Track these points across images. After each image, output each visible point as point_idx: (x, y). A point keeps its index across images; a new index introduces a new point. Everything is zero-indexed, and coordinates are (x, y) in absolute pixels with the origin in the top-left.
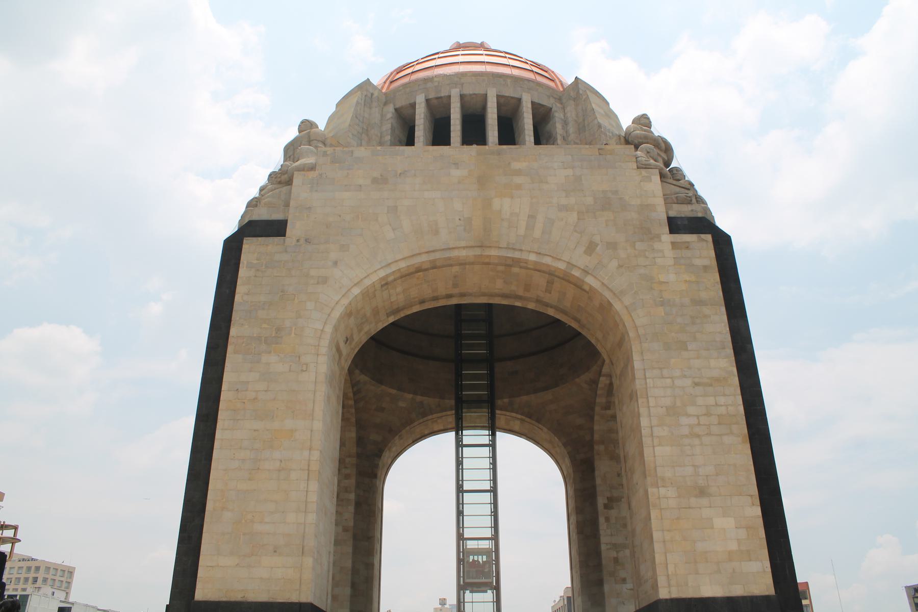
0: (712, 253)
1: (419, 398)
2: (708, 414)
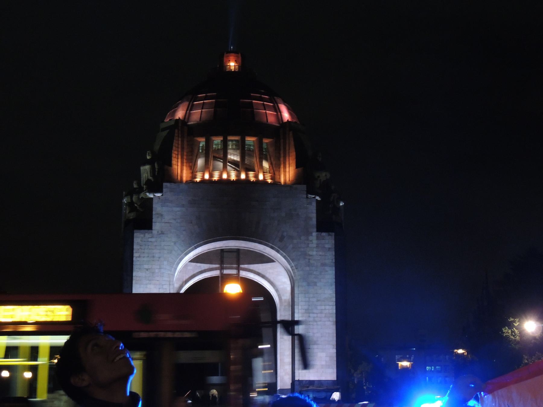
0: (333, 242)
1: (199, 264)
2: (321, 313)
